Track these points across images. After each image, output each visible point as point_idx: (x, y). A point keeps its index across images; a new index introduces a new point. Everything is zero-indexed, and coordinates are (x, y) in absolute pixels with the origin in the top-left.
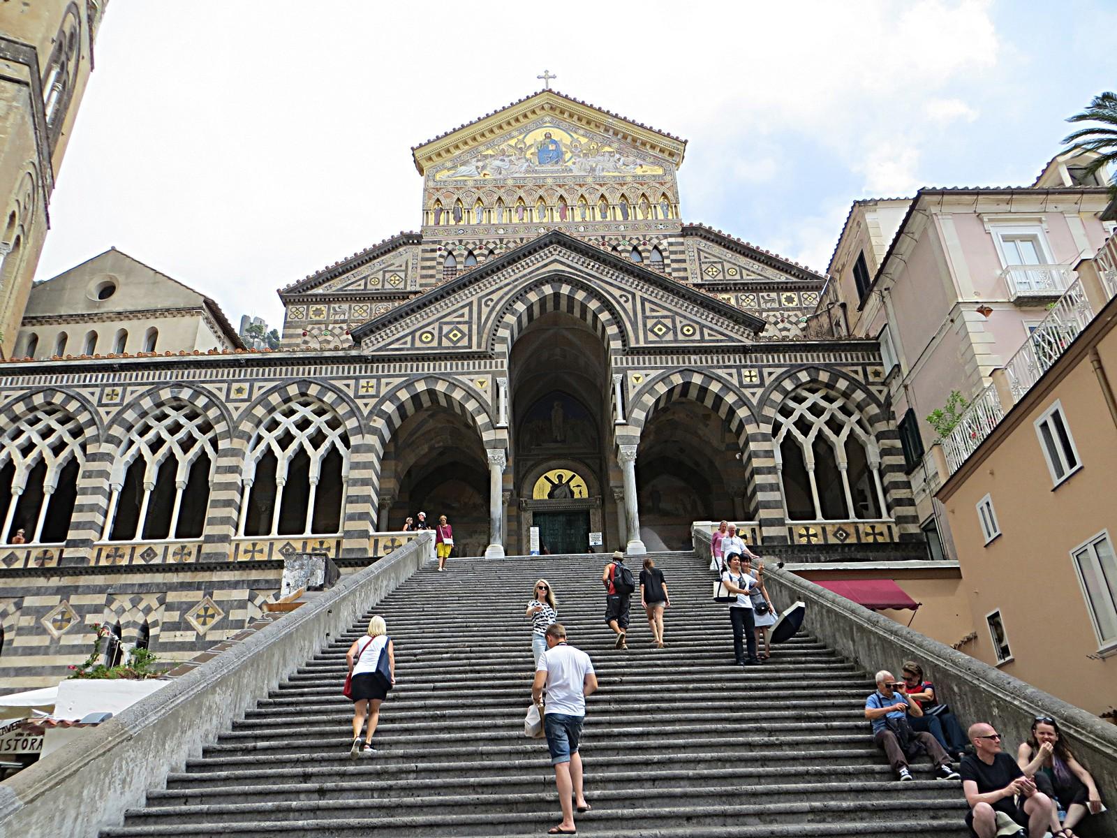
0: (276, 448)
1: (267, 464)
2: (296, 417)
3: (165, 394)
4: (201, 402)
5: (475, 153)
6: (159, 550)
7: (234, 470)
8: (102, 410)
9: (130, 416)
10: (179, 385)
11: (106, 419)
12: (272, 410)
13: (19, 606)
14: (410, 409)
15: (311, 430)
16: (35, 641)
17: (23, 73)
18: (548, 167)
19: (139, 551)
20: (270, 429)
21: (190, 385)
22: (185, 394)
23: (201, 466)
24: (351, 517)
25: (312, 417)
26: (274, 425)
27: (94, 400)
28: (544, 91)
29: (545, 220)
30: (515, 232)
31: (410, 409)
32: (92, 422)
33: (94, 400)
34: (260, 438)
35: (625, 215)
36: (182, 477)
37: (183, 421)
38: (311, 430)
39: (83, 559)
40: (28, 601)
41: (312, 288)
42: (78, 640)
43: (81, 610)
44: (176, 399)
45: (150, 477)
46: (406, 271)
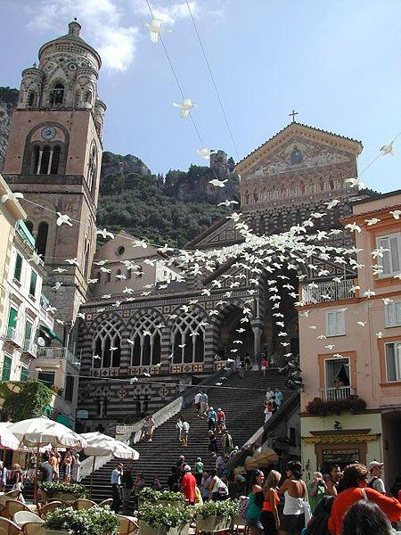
0: (180, 330)
1: (178, 336)
5: (262, 163)
7: (169, 340)
9: (133, 321)
14: (227, 311)
15: (192, 323)
16: (116, 400)
18: (296, 165)
21: (150, 308)
23: (157, 338)
24: (206, 357)
25: (192, 317)
29: (296, 195)
30: (281, 204)
31: (227, 311)
32: (121, 324)
35: (332, 187)
36: (151, 343)
38: (192, 323)
40: (112, 387)
42: (127, 400)
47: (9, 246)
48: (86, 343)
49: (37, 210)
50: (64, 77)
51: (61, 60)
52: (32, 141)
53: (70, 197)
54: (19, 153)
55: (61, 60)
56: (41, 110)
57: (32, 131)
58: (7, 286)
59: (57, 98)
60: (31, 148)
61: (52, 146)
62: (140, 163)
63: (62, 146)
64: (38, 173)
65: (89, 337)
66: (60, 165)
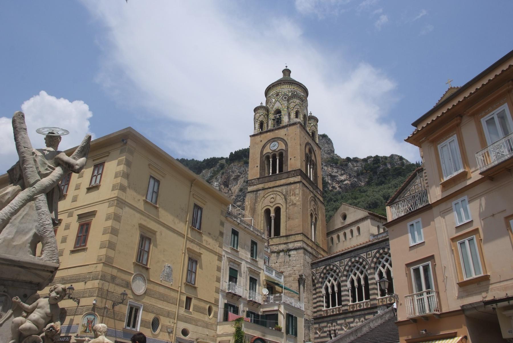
2: (385, 259)
3: (353, 260)
4: (361, 260)
6: (362, 304)
8: (341, 268)
9: (347, 268)
10: (355, 257)
11: (342, 270)
12: (378, 258)
13: (337, 324)
17: (298, 178)
19: (358, 305)
20: (379, 264)
22: (357, 259)
26: (380, 263)
27: (338, 265)
28: (449, 89)
32: (340, 272)
33: (338, 265)
34: (378, 267)
36: (363, 282)
37: (359, 266)
39: (346, 310)
40: (339, 322)
41: (395, 199)
43: (350, 323)
44: (355, 260)
45: (356, 284)
46: (421, 183)
47: (222, 224)
48: (318, 290)
49: (272, 200)
50: (280, 106)
51: (277, 95)
52: (264, 152)
53: (293, 186)
54: (257, 163)
55: (277, 95)
56: (267, 132)
57: (264, 147)
58: (223, 253)
59: (278, 121)
60: (264, 158)
61: (277, 154)
62: (401, 158)
63: (284, 155)
64: (271, 174)
65: (320, 285)
66: (284, 165)
